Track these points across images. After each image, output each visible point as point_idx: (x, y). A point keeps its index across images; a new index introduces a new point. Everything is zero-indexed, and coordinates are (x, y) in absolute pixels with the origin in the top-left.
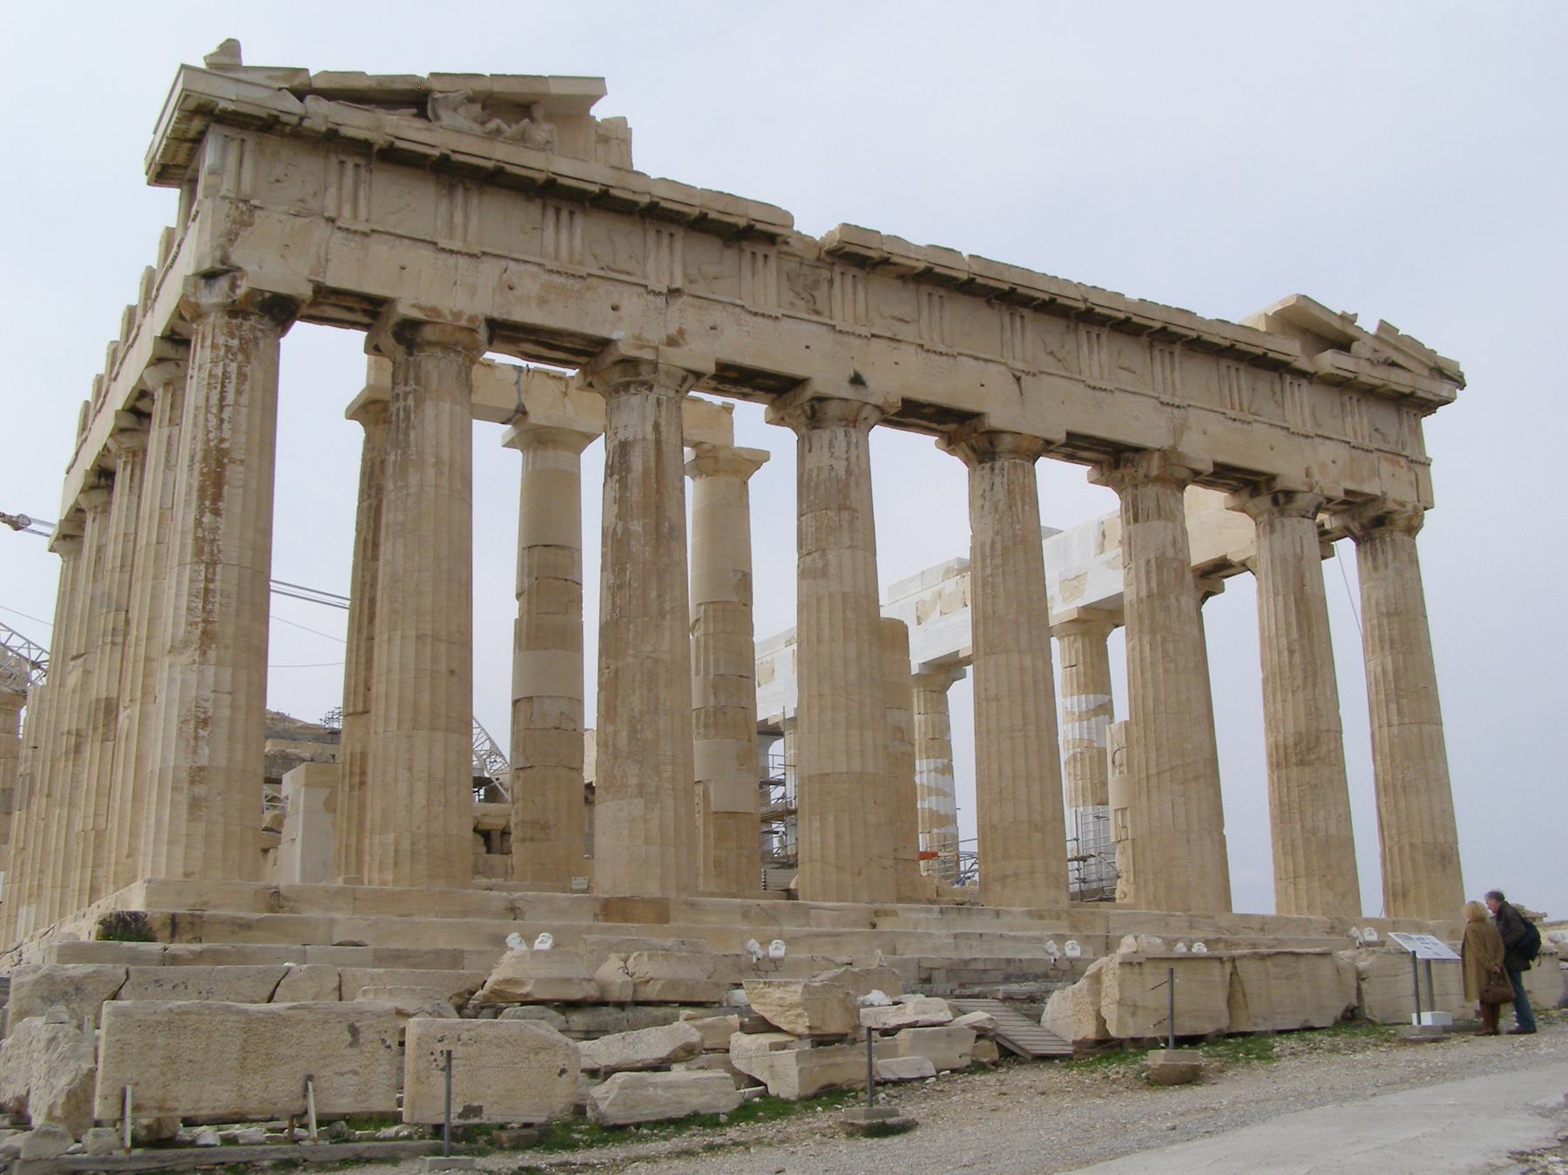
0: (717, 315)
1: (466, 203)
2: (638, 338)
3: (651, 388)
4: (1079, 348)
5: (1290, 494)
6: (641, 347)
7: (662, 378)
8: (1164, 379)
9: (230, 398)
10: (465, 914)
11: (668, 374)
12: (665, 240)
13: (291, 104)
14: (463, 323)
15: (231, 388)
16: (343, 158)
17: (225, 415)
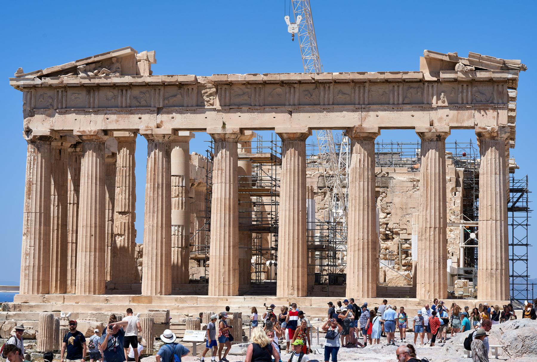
1: (94, 94)
2: (147, 127)
3: (154, 141)
4: (320, 94)
5: (422, 133)
6: (147, 130)
7: (155, 138)
8: (359, 98)
9: (32, 167)
10: (93, 301)
11: (157, 136)
12: (157, 91)
14: (92, 134)
15: (32, 164)
16: (58, 90)
17: (31, 171)
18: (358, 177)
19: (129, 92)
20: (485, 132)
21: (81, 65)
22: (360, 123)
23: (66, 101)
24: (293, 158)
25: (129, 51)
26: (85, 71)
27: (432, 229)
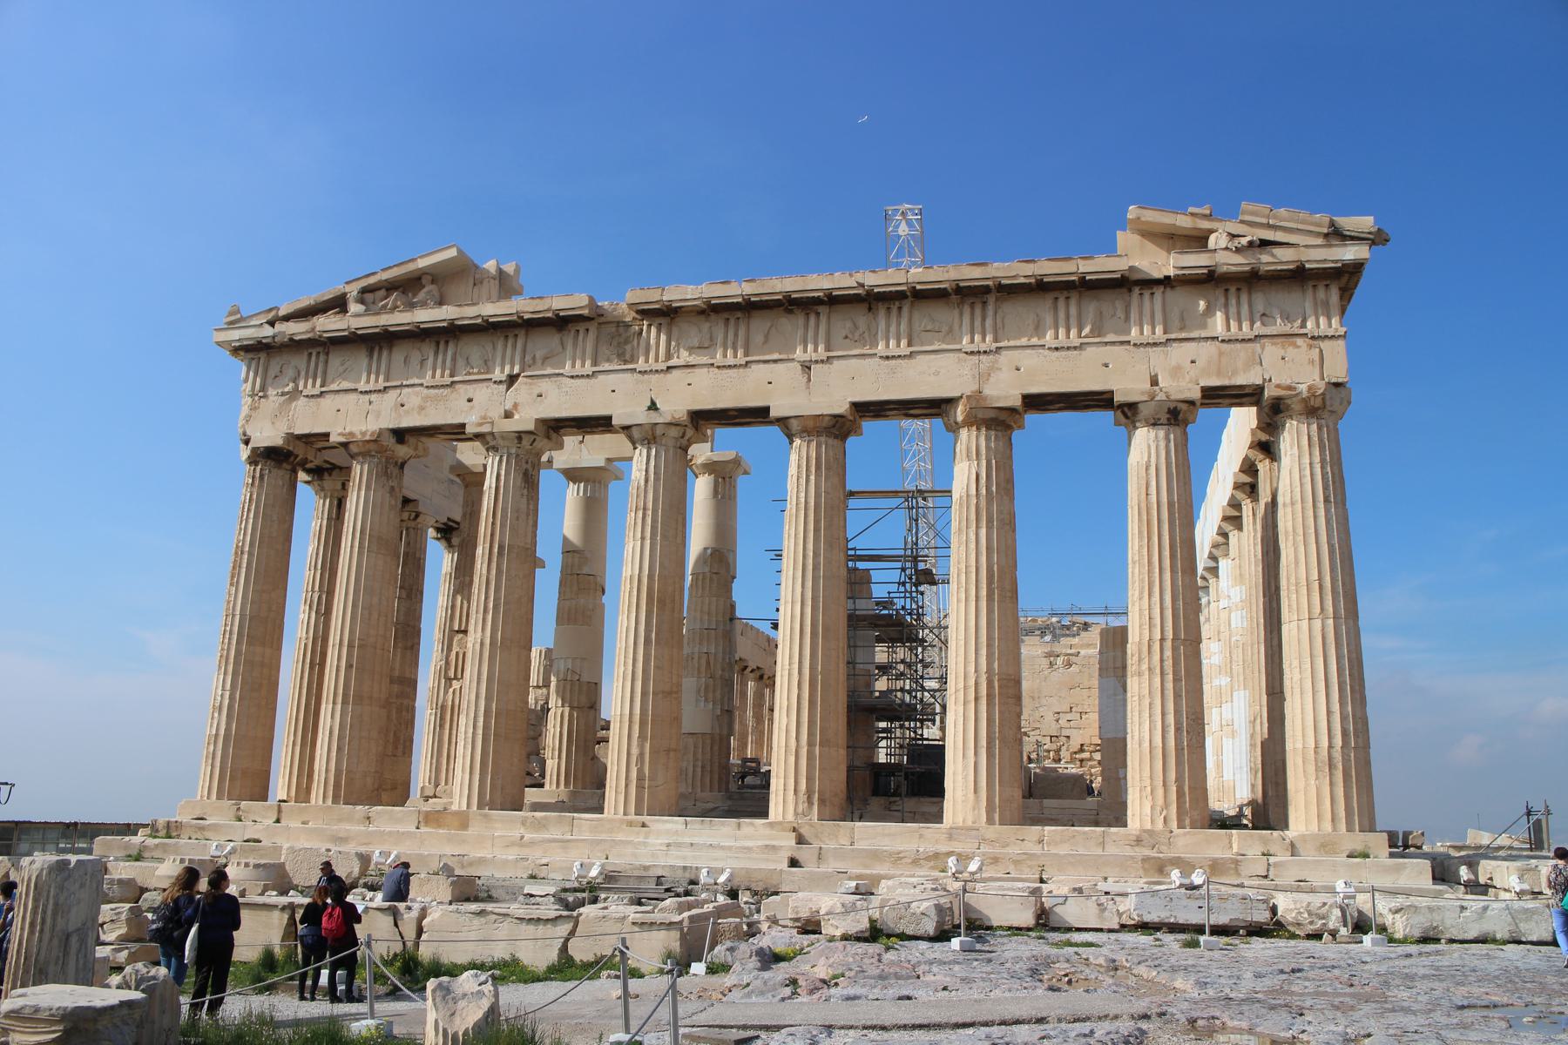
0: (544, 386)
2: (484, 418)
5: (1133, 406)
6: (481, 424)
7: (501, 442)
10: (340, 820)
11: (503, 438)
13: (268, 331)
18: (973, 516)
19: (451, 345)
20: (1291, 397)
21: (353, 290)
22: (976, 387)
23: (325, 373)
24: (812, 477)
25: (452, 253)
26: (361, 301)
27: (1168, 644)
